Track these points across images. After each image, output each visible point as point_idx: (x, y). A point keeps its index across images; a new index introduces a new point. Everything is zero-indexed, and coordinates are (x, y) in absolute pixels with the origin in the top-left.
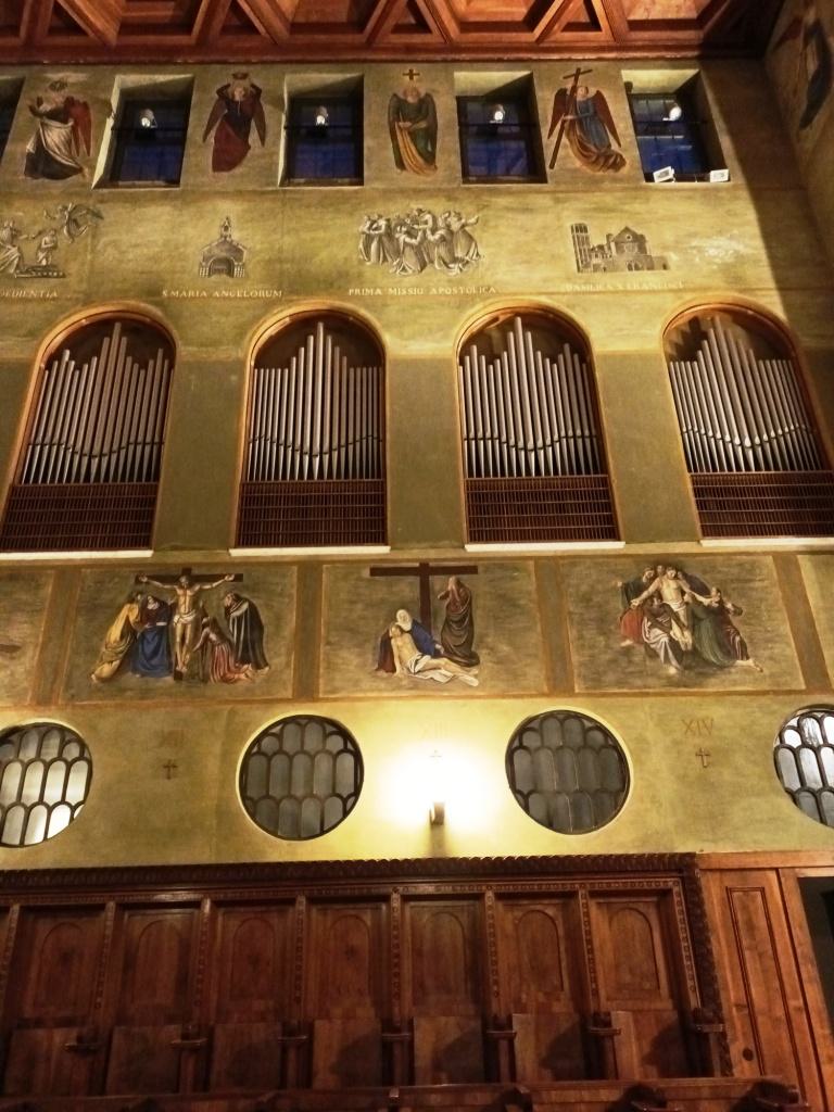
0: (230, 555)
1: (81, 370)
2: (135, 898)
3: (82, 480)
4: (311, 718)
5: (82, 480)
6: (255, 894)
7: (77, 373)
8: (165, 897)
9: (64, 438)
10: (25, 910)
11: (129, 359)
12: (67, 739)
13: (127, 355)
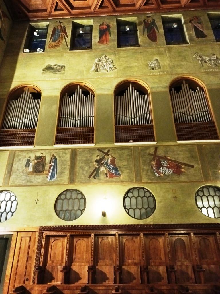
0: (177, 142)
1: (196, 92)
2: (170, 232)
3: (192, 122)
4: (210, 186)
5: (192, 122)
6: (206, 231)
7: (195, 93)
8: (178, 232)
9: (199, 110)
10: (95, 235)
11: (191, 90)
12: (132, 191)
13: (190, 89)
